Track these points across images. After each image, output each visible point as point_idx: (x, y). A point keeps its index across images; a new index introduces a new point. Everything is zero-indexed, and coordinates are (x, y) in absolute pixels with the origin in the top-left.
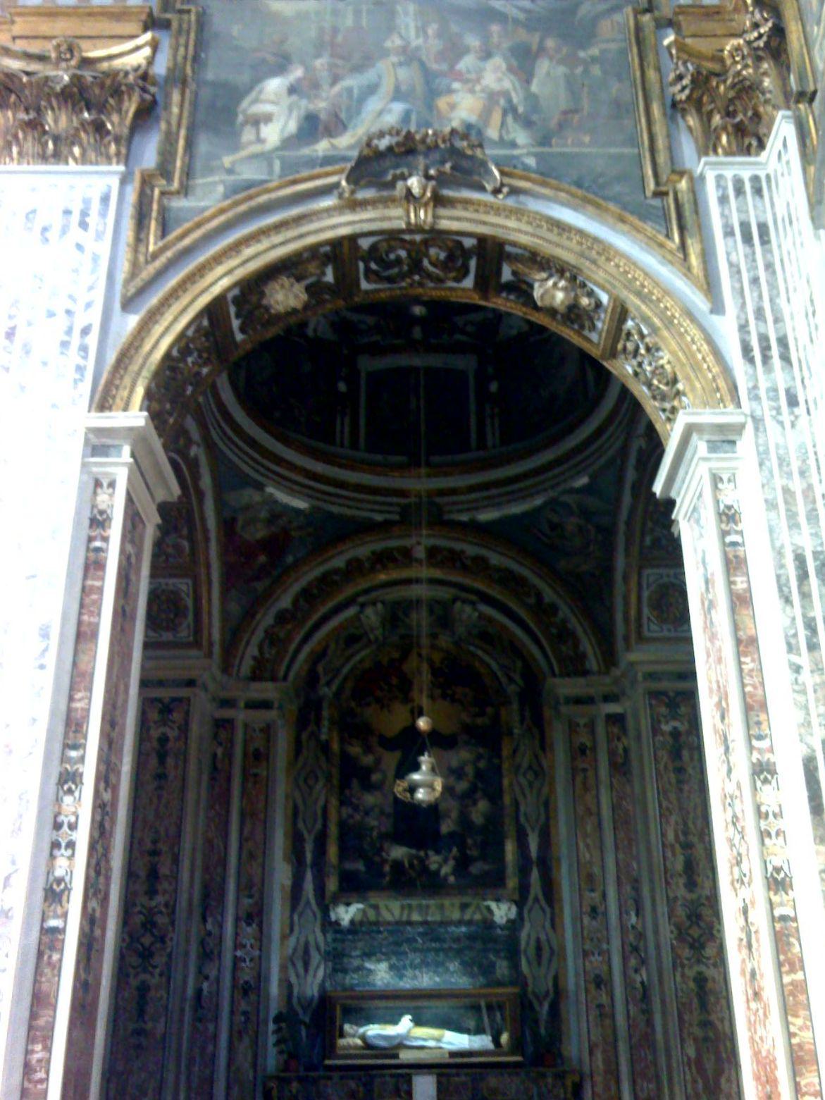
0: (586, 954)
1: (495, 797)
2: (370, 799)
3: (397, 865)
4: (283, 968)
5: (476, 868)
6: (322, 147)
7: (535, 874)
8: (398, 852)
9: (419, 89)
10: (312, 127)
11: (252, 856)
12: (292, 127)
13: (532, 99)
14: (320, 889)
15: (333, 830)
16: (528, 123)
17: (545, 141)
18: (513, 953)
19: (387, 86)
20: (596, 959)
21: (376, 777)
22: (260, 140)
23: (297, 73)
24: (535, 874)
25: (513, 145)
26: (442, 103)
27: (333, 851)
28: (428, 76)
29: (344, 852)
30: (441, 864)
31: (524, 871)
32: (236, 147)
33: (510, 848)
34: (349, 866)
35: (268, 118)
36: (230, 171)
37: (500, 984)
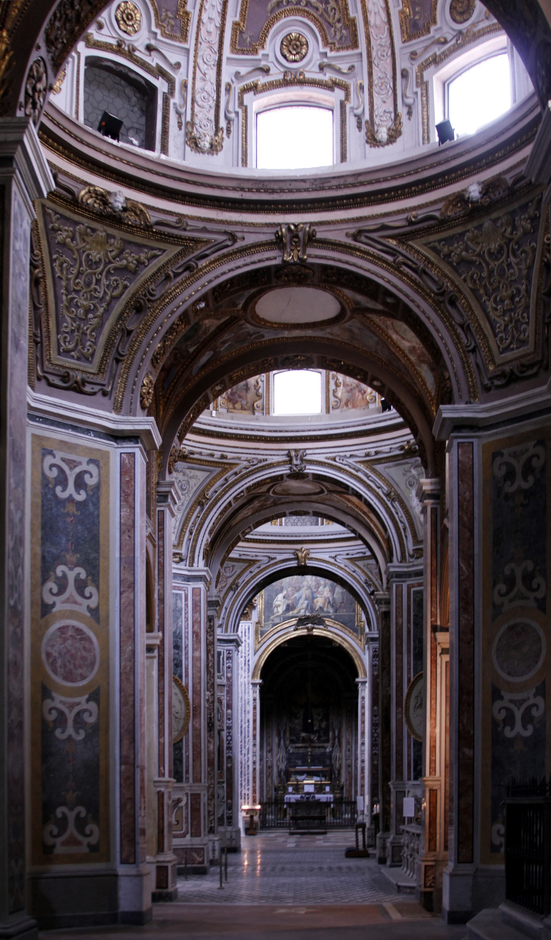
0: (346, 760)
1: (327, 720)
2: (297, 721)
3: (303, 738)
4: (277, 762)
5: (322, 739)
6: (291, 614)
7: (337, 740)
8: (303, 734)
9: (311, 597)
10: (289, 608)
11: (269, 737)
12: (284, 608)
13: (334, 599)
14: (285, 744)
15: (288, 729)
16: (333, 606)
17: (336, 611)
18: (330, 758)
19: (303, 597)
20: (349, 761)
21: (298, 716)
22: (278, 612)
23: (285, 592)
24: (337, 740)
25: (329, 612)
26: (315, 601)
27: (288, 735)
28: (313, 593)
29: (291, 734)
30: (314, 737)
31: (334, 739)
32: (273, 614)
33: (331, 734)
34: (292, 738)
35: (279, 606)
36: (273, 620)
37: (327, 766)
